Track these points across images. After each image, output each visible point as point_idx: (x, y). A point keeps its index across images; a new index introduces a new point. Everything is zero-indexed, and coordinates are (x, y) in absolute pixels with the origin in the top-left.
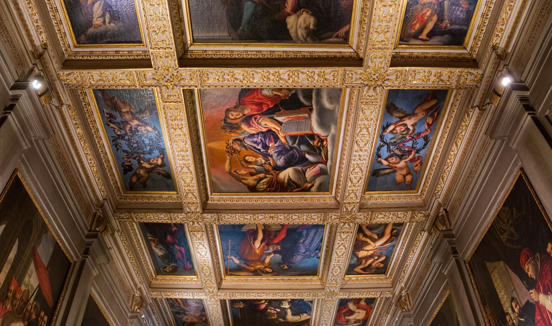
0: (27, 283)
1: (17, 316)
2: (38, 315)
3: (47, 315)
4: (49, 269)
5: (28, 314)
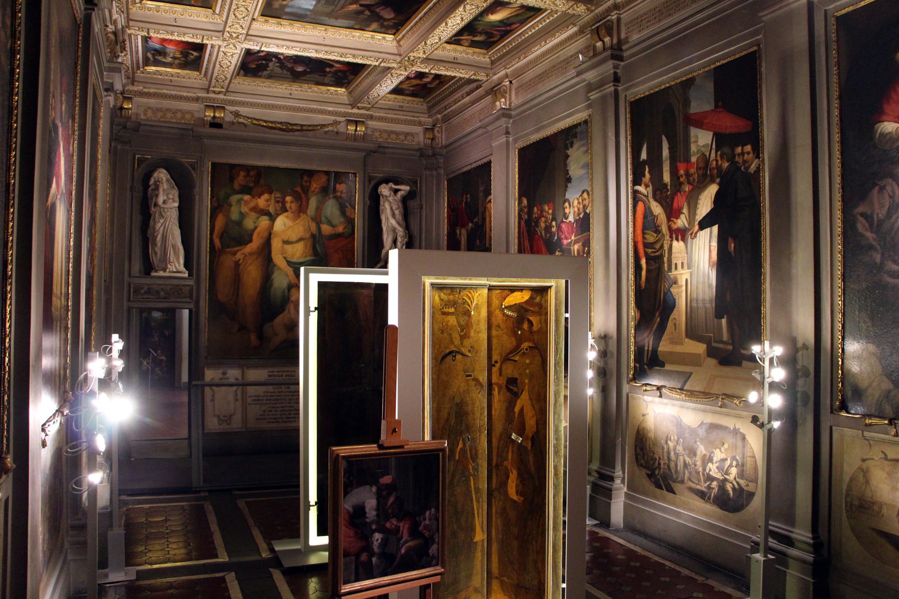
2: (732, 159)
4: (720, 104)
5: (715, 171)
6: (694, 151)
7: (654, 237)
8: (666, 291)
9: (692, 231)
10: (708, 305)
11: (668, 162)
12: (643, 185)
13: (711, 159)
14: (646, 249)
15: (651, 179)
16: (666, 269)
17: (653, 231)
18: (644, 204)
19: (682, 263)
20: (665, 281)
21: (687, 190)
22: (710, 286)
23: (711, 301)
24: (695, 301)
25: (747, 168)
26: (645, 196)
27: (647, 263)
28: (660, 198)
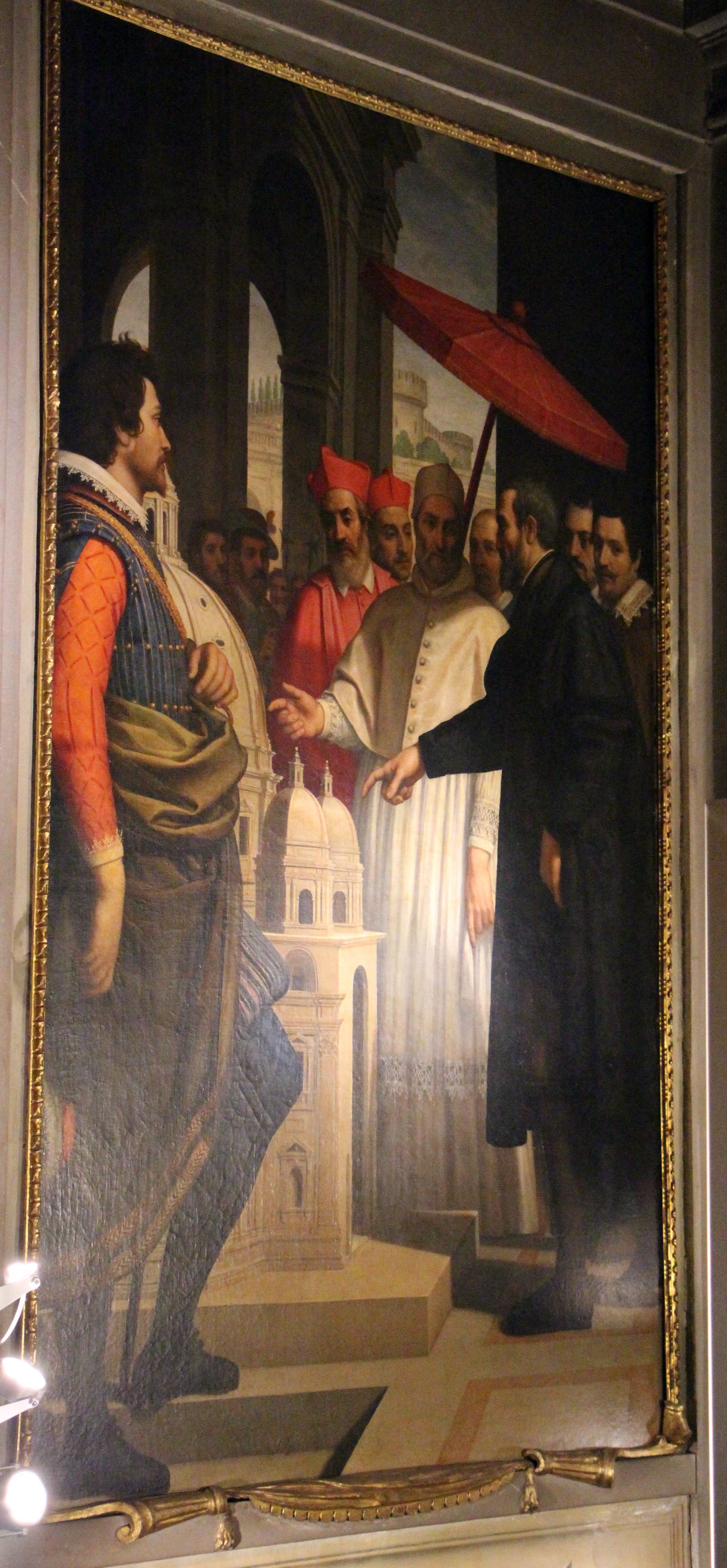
0: (414, 439)
1: (435, 592)
3: (612, 514)
4: (520, 308)
5: (494, 560)
6: (404, 436)
7: (180, 742)
8: (248, 1014)
9: (388, 767)
10: (457, 1090)
11: (278, 422)
12: (119, 466)
13: (476, 510)
14: (129, 796)
15: (171, 457)
16: (251, 912)
17: (171, 713)
18: (125, 564)
19: (340, 899)
20: (240, 966)
21: (369, 583)
22: (466, 1010)
23: (469, 1069)
24: (402, 1070)
25: (614, 599)
26: (134, 527)
27: (128, 860)
28: (222, 569)
